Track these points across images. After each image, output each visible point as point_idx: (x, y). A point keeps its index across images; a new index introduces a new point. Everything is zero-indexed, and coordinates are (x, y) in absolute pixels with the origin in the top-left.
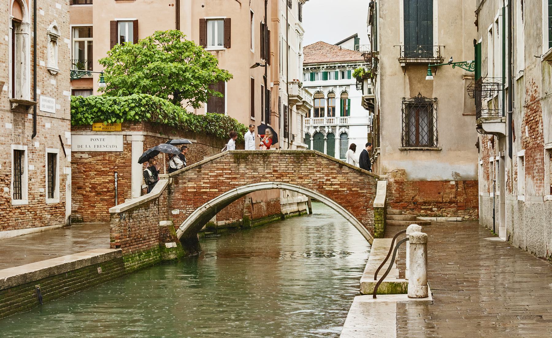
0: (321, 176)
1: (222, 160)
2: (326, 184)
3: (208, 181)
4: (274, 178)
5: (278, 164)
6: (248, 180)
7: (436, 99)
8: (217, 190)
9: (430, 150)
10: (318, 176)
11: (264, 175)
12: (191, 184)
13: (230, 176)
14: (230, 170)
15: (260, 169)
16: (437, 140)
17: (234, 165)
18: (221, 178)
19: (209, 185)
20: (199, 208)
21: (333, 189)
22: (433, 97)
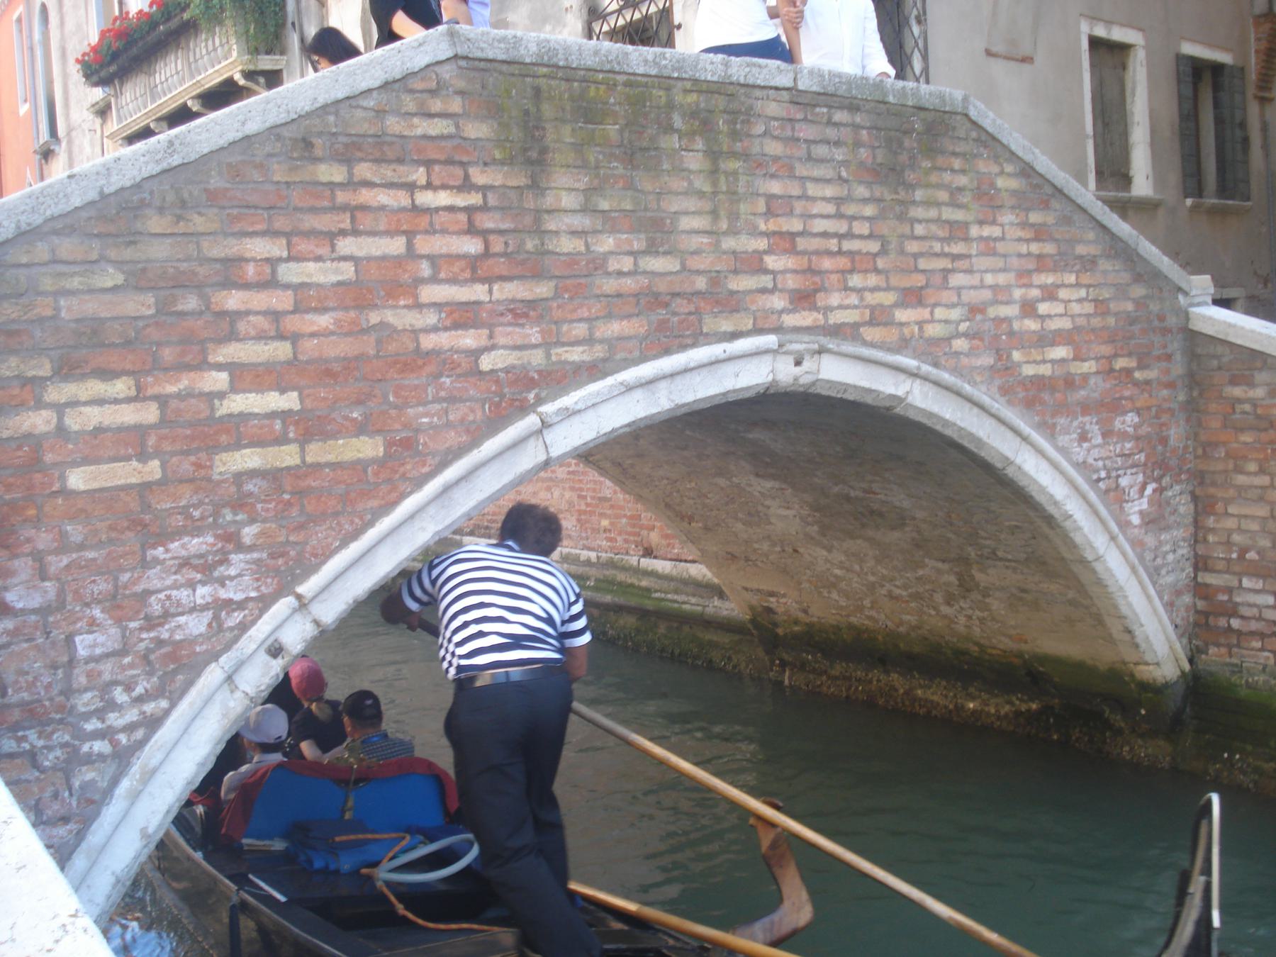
1: (394, 124)
3: (282, 350)
4: (778, 302)
6: (615, 328)
8: (368, 448)
10: (989, 279)
12: (102, 404)
13: (478, 292)
14: (471, 230)
18: (400, 317)
19: (289, 401)
20: (213, 675)
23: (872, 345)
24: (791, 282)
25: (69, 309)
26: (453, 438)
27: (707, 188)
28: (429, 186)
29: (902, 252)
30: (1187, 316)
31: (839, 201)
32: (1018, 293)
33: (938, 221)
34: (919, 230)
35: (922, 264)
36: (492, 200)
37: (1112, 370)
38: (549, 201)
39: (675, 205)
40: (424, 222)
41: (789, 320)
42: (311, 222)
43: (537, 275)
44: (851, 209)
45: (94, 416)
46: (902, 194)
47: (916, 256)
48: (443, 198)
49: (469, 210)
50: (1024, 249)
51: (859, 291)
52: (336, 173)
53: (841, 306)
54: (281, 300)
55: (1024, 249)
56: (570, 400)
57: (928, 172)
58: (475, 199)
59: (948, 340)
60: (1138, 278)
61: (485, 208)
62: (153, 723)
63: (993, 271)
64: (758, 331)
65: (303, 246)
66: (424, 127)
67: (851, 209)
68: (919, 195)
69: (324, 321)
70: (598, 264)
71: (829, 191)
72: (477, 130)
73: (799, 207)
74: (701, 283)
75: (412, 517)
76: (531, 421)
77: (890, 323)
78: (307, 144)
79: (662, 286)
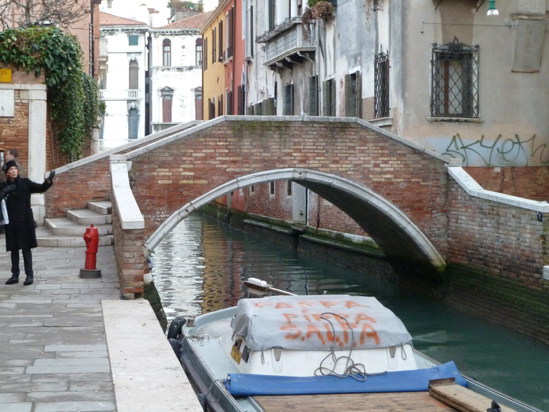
0: (367, 159)
1: (213, 132)
2: (373, 173)
3: (192, 166)
4: (295, 162)
5: (302, 140)
6: (255, 165)
7: (477, 46)
8: (204, 182)
9: (470, 122)
10: (362, 158)
11: (279, 158)
12: (164, 172)
13: (227, 158)
14: (227, 148)
15: (274, 147)
16: (477, 107)
17: (232, 140)
18: (212, 162)
19: (193, 174)
21: (383, 180)
22: (474, 43)
23: (322, 171)
24: (299, 158)
25: (160, 159)
26: (220, 182)
27: (279, 141)
28: (219, 141)
29: (333, 152)
30: (447, 169)
31: (314, 142)
32: (372, 162)
33: (346, 146)
34: (338, 148)
35: (339, 155)
36: (231, 143)
37: (410, 181)
38: (242, 143)
39: (270, 144)
40: (218, 147)
41: (297, 166)
42: (199, 147)
43: (239, 156)
44: (317, 144)
45: (163, 174)
46: (334, 140)
47: (337, 153)
48: (222, 143)
49: (227, 145)
50: (376, 152)
51: (319, 160)
52: (203, 140)
53: (312, 163)
54: (192, 159)
55: (376, 152)
56: (243, 177)
57: (343, 135)
58: (228, 143)
59: (347, 171)
60: (424, 159)
61: (229, 145)
62: (167, 218)
63: (364, 157)
64: (289, 167)
65: (196, 151)
66: (221, 132)
67: (317, 144)
68: (339, 140)
69: (199, 162)
70: (252, 154)
71: (311, 140)
72: (229, 132)
73: (302, 144)
74: (276, 158)
75: (211, 193)
76: (235, 180)
77: (327, 167)
78: (198, 135)
79: (266, 158)
